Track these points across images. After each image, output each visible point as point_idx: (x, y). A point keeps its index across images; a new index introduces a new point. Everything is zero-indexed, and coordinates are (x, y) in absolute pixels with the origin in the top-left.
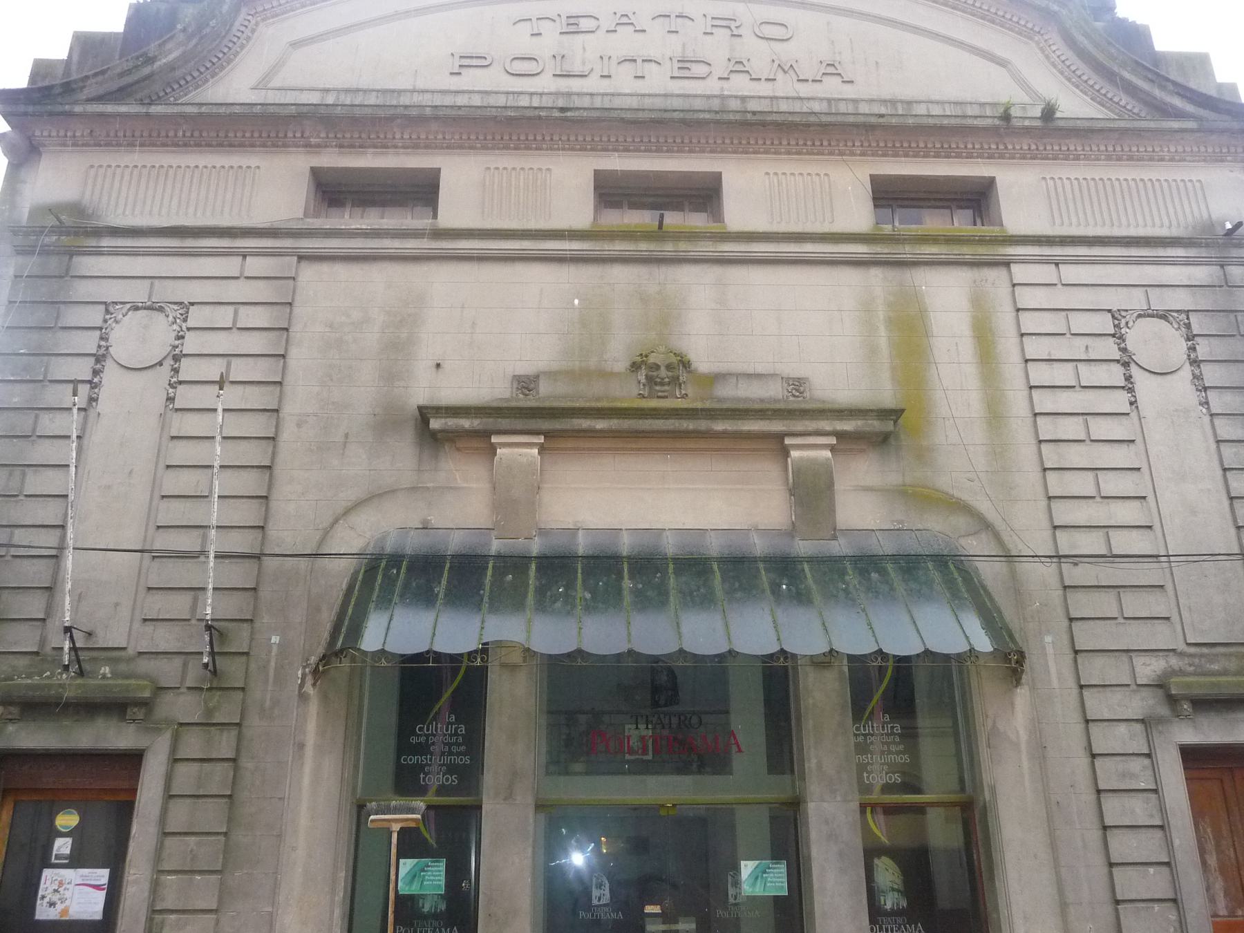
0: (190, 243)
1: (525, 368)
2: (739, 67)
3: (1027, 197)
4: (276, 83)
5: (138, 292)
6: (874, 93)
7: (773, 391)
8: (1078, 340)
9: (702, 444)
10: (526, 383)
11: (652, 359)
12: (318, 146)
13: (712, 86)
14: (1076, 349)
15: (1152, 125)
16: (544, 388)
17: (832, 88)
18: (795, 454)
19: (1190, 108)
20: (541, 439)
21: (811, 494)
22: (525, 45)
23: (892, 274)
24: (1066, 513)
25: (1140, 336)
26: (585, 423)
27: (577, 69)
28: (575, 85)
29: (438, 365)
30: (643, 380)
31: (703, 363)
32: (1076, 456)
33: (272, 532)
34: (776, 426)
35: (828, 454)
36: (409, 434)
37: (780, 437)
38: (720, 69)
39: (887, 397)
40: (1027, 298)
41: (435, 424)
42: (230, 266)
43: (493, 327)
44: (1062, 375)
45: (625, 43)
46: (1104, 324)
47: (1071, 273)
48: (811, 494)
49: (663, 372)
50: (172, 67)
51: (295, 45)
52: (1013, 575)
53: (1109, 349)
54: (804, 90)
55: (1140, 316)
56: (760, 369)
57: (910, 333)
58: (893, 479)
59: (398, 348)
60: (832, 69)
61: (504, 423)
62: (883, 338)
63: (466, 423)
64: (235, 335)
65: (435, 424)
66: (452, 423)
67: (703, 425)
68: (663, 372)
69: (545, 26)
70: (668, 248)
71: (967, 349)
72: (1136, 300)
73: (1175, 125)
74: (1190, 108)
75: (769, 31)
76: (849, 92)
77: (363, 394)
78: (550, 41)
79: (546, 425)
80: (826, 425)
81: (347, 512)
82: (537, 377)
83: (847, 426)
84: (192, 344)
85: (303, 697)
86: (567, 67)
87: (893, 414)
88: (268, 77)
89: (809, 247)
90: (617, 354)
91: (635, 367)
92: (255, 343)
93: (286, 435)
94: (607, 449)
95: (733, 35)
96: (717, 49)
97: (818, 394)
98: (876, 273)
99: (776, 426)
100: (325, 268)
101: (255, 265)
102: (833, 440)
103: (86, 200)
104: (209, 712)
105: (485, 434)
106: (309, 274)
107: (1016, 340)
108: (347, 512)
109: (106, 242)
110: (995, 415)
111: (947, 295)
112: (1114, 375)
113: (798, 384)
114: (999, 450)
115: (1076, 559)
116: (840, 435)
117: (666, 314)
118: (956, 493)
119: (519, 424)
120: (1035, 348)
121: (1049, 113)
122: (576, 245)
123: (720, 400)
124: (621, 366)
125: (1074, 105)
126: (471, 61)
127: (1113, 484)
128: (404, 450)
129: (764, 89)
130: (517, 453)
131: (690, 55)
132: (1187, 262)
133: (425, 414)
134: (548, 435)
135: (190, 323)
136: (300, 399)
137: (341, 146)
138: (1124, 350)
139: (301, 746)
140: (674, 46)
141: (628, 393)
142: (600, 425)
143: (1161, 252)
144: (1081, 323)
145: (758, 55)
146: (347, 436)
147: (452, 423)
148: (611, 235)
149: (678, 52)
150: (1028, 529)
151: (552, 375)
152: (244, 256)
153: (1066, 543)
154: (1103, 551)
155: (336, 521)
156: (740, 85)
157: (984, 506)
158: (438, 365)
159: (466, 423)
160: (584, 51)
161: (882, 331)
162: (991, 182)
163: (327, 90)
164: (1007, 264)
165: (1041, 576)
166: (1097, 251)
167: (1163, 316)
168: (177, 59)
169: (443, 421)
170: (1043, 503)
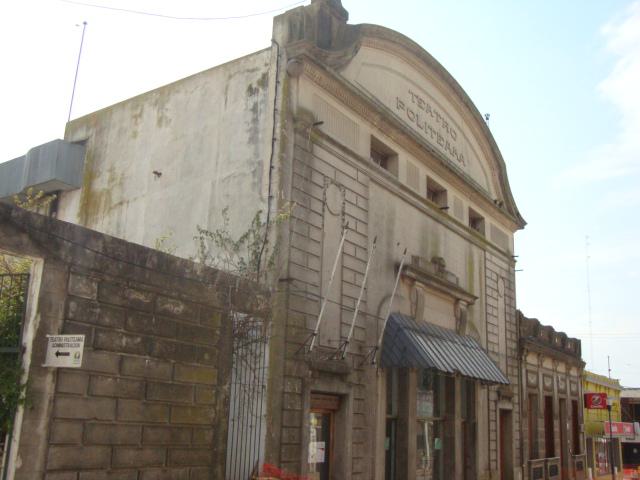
0: (346, 156)
7: (452, 280)
9: (443, 296)
10: (416, 259)
17: (460, 165)
34: (458, 295)
41: (408, 273)
42: (351, 171)
43: (409, 230)
45: (432, 122)
46: (495, 277)
47: (494, 259)
48: (461, 320)
69: (415, 100)
83: (469, 300)
85: (377, 376)
104: (360, 380)
105: (413, 280)
106: (373, 187)
117: (436, 245)
124: (429, 260)
130: (419, 286)
132: (501, 259)
134: (427, 285)
139: (377, 395)
141: (432, 269)
142: (435, 285)
162: (482, 219)
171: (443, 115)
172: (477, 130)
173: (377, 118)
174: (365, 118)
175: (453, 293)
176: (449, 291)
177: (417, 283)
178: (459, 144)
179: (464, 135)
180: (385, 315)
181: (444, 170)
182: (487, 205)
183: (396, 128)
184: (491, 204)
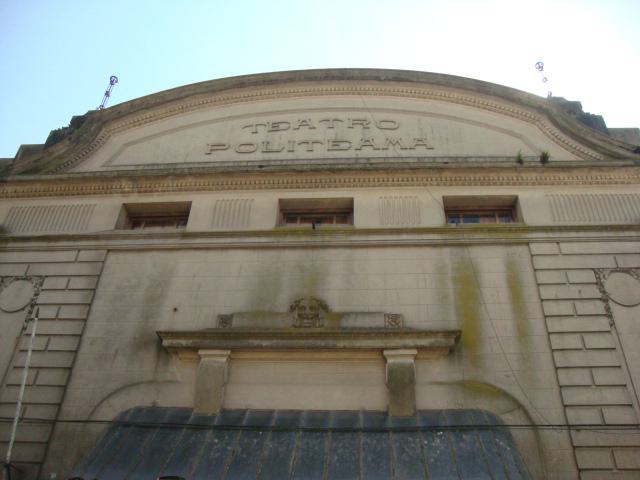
0: (52, 244)
1: (224, 311)
2: (367, 143)
3: (536, 202)
4: (114, 164)
5: (20, 271)
6: (445, 153)
7: (379, 322)
8: (573, 288)
10: (225, 319)
11: (302, 304)
12: (128, 192)
13: (352, 154)
14: (573, 292)
15: (607, 163)
16: (236, 323)
17: (421, 152)
18: (390, 361)
19: (629, 154)
20: (229, 352)
21: (400, 384)
22: (246, 136)
23: (455, 250)
24: (572, 397)
25: (612, 283)
26: (256, 342)
27: (275, 148)
28: (273, 156)
29: (175, 310)
30: (296, 316)
31: (336, 306)
32: (576, 359)
33: (65, 408)
34: (378, 343)
35: (411, 360)
36: (153, 349)
37: (381, 350)
38: (356, 143)
39: (453, 324)
40: (541, 263)
41: (166, 343)
42: (71, 256)
44: (565, 308)
45: (304, 134)
46: (591, 277)
47: (566, 247)
48: (400, 384)
49: (308, 311)
50: (61, 157)
51: (127, 145)
52: (538, 439)
53: (595, 292)
54: (404, 153)
55: (612, 272)
56: (372, 309)
57: (468, 285)
58: (457, 376)
59: (154, 300)
60: (420, 142)
61: (207, 342)
62: (450, 290)
63: (184, 342)
64: (66, 293)
65: (166, 343)
66: (176, 342)
67: (331, 342)
68: (308, 311)
70: (318, 240)
71: (504, 295)
72: (609, 263)
73: (621, 163)
74: (629, 154)
75: (384, 125)
76: (430, 153)
77: (131, 326)
78: (263, 134)
79: (233, 343)
80: (410, 342)
81: (109, 396)
82: (232, 316)
83: (424, 342)
84: (41, 299)
86: (270, 147)
87: (456, 335)
88: (110, 160)
89: (404, 237)
90: (282, 302)
91: (292, 309)
92: (75, 298)
93: (83, 350)
94: (271, 359)
95: (364, 128)
96: (355, 135)
97: (408, 324)
98: (446, 250)
99: (378, 343)
100: (121, 256)
101: (84, 255)
102: (415, 352)
103: (6, 225)
107: (534, 288)
108: (109, 396)
109: (10, 245)
110: (523, 334)
111: (491, 262)
112: (600, 307)
113: (395, 317)
114: (526, 357)
115: (578, 428)
116: (420, 348)
118: (499, 385)
119: (216, 343)
120: (546, 293)
121: (544, 158)
122: (263, 240)
123: (344, 328)
124: (284, 308)
125: (558, 154)
126: (217, 147)
127: (602, 377)
128: (149, 358)
129: (382, 154)
130: (215, 358)
131: (339, 138)
133: (161, 335)
134: (234, 350)
135: (43, 287)
136: (96, 328)
137: (139, 192)
138: (604, 292)
140: (331, 134)
141: (286, 323)
142: (265, 343)
143: (621, 234)
144: (574, 277)
145: (378, 136)
146: (117, 351)
147: (176, 342)
148: (285, 233)
149: (333, 137)
150: (546, 406)
151: (241, 314)
152: (79, 251)
153: (573, 417)
154: (600, 422)
155: (102, 402)
156: (368, 152)
157: (517, 393)
158: (175, 310)
159: (184, 342)
160: (280, 139)
161: (450, 285)
162: (515, 200)
163: (139, 165)
164: (528, 244)
165: (556, 440)
166: (582, 234)
167: (627, 271)
168: (64, 153)
169: (170, 341)
170: (556, 390)
171: (253, 121)
172: (456, 95)
173: (436, 171)
174: (108, 192)
175: (341, 344)
176: (322, 343)
177: (200, 352)
178: (408, 129)
179: (404, 112)
180: (109, 412)
181: (313, 178)
182: (504, 175)
183: (165, 176)
184: (534, 169)
